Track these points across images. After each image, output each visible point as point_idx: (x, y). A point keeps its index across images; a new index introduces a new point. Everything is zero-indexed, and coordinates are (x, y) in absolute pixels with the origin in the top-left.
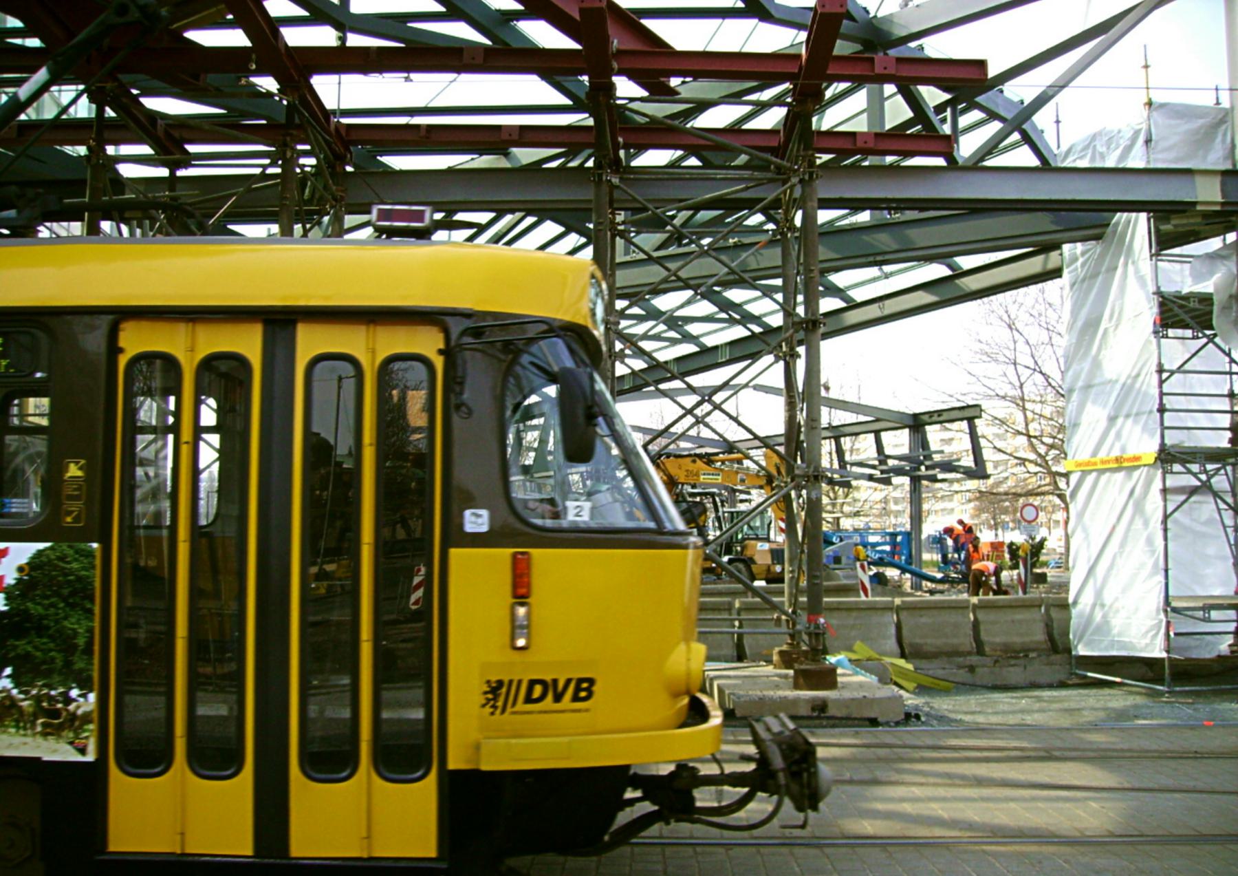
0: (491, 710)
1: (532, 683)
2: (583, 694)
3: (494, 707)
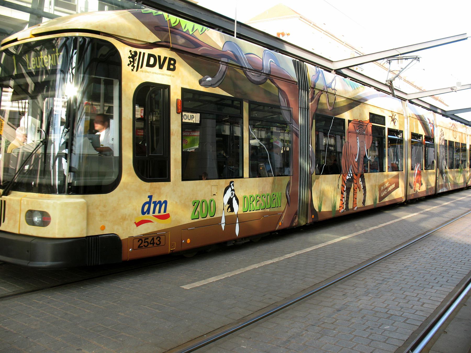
0: (132, 68)
1: (150, 56)
2: (172, 67)
3: (133, 66)
